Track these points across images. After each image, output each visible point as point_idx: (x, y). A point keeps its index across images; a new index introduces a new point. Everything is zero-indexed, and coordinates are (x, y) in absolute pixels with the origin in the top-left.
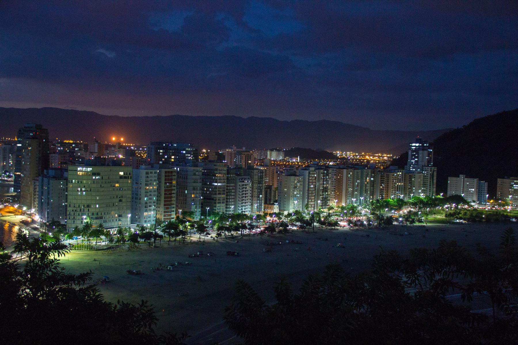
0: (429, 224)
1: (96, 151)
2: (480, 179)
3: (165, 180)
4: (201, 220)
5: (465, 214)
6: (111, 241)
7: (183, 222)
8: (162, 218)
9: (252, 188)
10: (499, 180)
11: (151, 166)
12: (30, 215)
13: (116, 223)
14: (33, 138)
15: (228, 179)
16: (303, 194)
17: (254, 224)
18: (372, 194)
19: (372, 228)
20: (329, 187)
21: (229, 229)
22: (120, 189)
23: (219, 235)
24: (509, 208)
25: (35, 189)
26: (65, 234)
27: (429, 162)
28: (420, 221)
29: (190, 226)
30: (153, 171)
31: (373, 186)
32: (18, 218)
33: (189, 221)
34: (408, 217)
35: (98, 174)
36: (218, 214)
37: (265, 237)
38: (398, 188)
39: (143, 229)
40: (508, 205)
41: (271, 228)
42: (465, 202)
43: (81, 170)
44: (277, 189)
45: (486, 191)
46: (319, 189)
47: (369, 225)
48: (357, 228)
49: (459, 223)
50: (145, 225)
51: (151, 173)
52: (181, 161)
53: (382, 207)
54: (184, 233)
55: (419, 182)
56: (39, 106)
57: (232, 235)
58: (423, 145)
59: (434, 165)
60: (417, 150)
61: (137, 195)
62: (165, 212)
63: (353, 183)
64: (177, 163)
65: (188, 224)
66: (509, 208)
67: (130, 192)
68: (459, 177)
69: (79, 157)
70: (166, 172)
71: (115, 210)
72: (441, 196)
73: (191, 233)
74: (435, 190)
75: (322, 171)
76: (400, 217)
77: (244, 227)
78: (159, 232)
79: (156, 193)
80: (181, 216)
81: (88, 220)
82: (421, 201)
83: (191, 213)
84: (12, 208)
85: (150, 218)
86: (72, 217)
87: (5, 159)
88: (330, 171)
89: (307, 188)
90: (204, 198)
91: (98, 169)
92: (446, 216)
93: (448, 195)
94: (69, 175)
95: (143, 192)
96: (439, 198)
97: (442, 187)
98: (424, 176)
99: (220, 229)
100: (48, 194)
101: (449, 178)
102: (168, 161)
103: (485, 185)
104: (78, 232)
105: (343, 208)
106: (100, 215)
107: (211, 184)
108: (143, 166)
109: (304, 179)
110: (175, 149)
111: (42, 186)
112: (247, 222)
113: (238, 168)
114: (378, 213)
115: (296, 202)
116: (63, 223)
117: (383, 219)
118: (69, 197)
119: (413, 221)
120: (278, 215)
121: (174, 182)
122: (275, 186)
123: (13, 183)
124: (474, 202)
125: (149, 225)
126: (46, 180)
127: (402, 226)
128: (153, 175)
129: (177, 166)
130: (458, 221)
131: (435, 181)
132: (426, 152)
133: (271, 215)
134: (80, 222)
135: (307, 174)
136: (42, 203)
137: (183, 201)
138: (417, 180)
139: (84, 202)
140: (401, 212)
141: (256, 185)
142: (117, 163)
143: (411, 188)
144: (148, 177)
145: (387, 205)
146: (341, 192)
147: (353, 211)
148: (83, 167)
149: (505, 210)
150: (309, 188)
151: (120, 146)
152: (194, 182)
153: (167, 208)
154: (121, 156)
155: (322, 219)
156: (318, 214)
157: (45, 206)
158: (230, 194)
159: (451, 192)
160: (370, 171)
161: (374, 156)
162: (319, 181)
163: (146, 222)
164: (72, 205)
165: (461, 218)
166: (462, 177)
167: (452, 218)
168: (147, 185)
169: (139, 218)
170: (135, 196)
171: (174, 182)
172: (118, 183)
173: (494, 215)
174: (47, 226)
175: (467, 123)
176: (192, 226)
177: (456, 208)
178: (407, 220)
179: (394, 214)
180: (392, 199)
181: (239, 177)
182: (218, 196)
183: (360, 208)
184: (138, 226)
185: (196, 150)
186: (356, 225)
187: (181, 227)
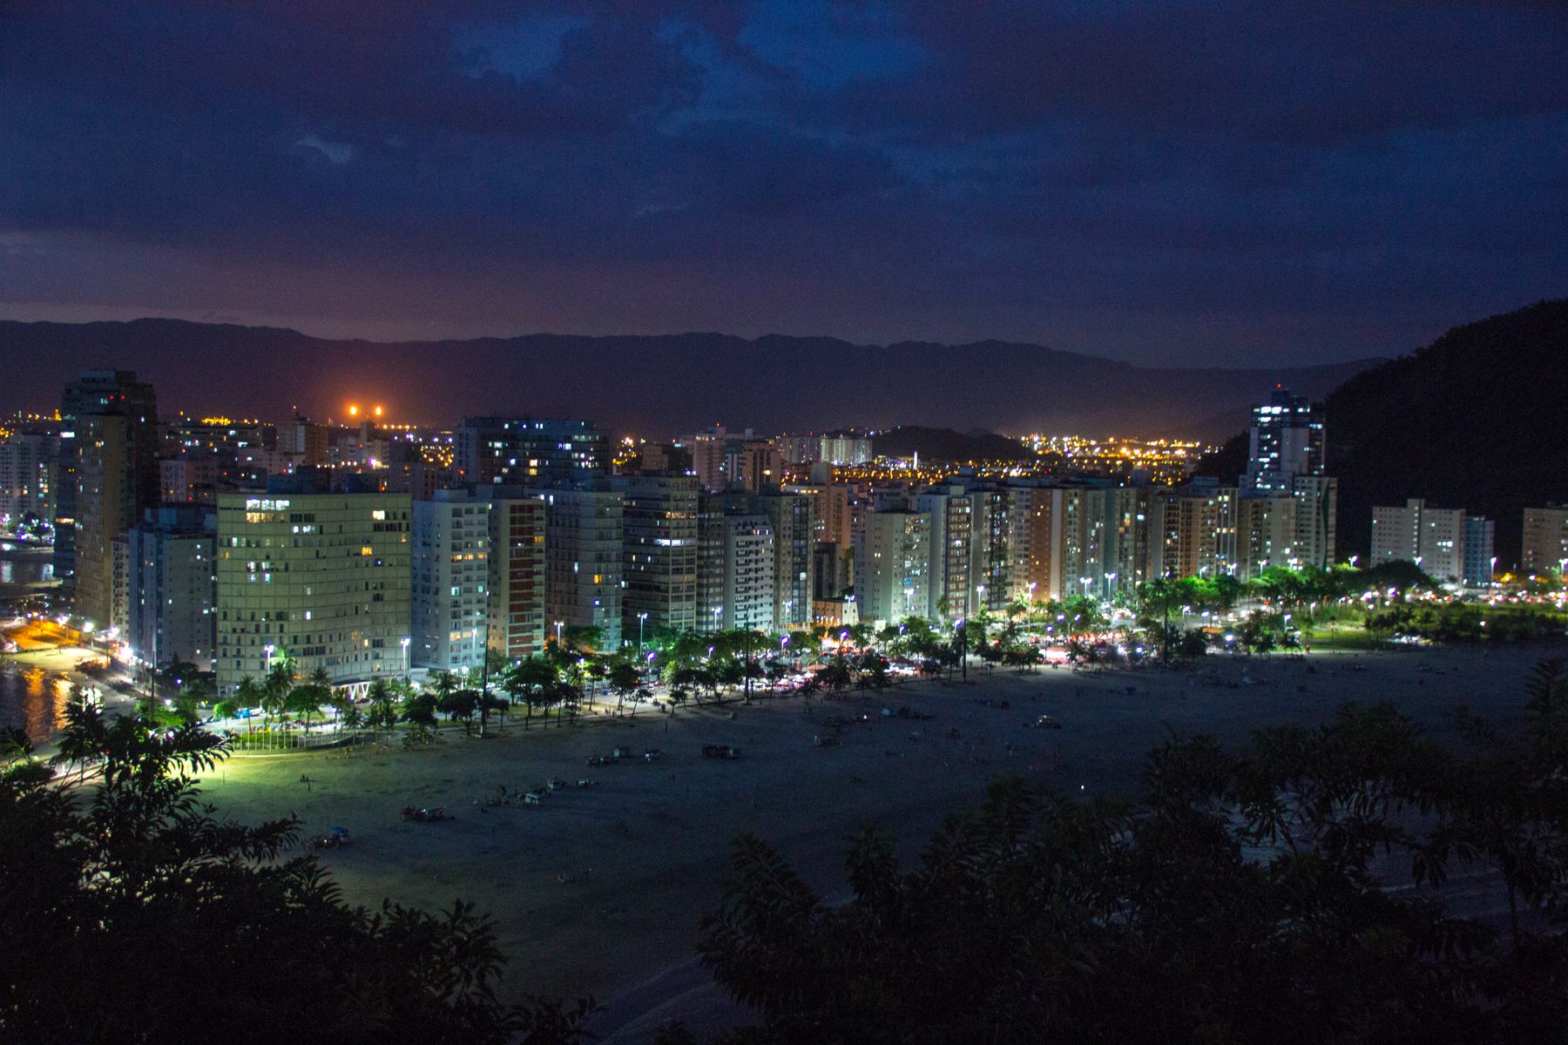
0: (1314, 652)
1: (302, 449)
2: (1471, 513)
3: (513, 532)
4: (622, 651)
5: (1427, 618)
6: (352, 719)
7: (568, 659)
8: (506, 648)
9: (777, 550)
10: (1529, 515)
11: (469, 489)
12: (106, 647)
13: (366, 667)
14: (110, 411)
15: (701, 526)
16: (932, 568)
17: (785, 660)
18: (1142, 562)
19: (1142, 667)
21: (707, 679)
22: (374, 561)
23: (678, 696)
25: (118, 566)
26: (213, 702)
27: (1313, 461)
28: (1289, 643)
29: (590, 669)
30: (475, 506)
31: (1144, 539)
32: (68, 658)
33: (588, 657)
34: (1249, 632)
35: (309, 519)
36: (674, 631)
37: (819, 696)
38: (1221, 545)
39: (447, 681)
40: (1557, 588)
41: (836, 672)
43: (257, 507)
44: (851, 552)
45: (1489, 548)
46: (978, 553)
47: (1134, 657)
48: (1096, 666)
49: (1409, 645)
50: (454, 671)
51: (469, 511)
52: (560, 473)
53: (1172, 602)
54: (572, 692)
56: (126, 315)
57: (718, 695)
58: (1294, 413)
59: (1328, 472)
60: (1276, 427)
61: (426, 578)
62: (512, 630)
63: (1084, 533)
64: (546, 481)
65: (582, 664)
67: (406, 572)
68: (1404, 505)
69: (249, 469)
70: (513, 509)
71: (361, 628)
72: (1350, 565)
73: (593, 692)
74: (1332, 546)
75: (987, 496)
76: (1228, 630)
77: (754, 670)
78: (496, 690)
79: (485, 573)
80: (561, 642)
81: (281, 658)
82: (1291, 583)
83: (593, 633)
84: (50, 626)
85: (468, 647)
86: (232, 651)
87: (25, 477)
88: (1012, 496)
89: (942, 550)
90: (631, 587)
91: (308, 503)
92: (1367, 625)
93: (1373, 563)
94: (222, 522)
95: (444, 570)
96: (1347, 573)
97: (1353, 536)
98: (1299, 506)
99: (681, 677)
100: (160, 582)
101: (1376, 510)
102: (518, 474)
103: (1485, 528)
104: (249, 695)
105: (1053, 608)
106: (315, 643)
107: (650, 543)
108: (445, 493)
109: (933, 522)
110: (539, 437)
111: (140, 557)
112: (763, 655)
113: (732, 491)
114: (1160, 620)
115: (910, 592)
116: (205, 668)
117: (1177, 640)
118: (222, 590)
119: (1267, 644)
120: (856, 632)
121: (539, 539)
122: (847, 543)
123: (51, 550)
124: (1453, 580)
125: (465, 670)
126: (149, 539)
127: (1234, 659)
128: (475, 518)
129: (548, 488)
130: (1404, 640)
131: (1332, 521)
132: (1303, 433)
133: (835, 633)
134: (255, 664)
135: (943, 507)
136: (140, 608)
137: (568, 598)
138: (1278, 516)
139: (268, 604)
140: (1231, 617)
141: (786, 544)
142: (364, 484)
143: (1259, 544)
144: (458, 525)
145: (1188, 595)
146: (1045, 557)
147: (1085, 615)
148: (261, 497)
149: (1549, 605)
150: (948, 548)
151: (372, 432)
152: (601, 538)
153: (520, 619)
154: (376, 463)
155: (992, 643)
156: (978, 627)
157: (150, 619)
158: (708, 573)
159: (1383, 552)
160: (1133, 492)
162: (978, 527)
163: (455, 660)
164: (232, 615)
165: (1413, 632)
166: (1414, 505)
167: (1386, 631)
168: (456, 549)
169: (436, 649)
170: (420, 583)
171: (539, 539)
172: (368, 543)
173: (1514, 620)
174: (156, 678)
176: (597, 671)
177: (1399, 599)
178: (1248, 640)
179: (1212, 622)
180: (1201, 577)
181: (733, 521)
182: (674, 578)
183: (1104, 606)
184: (432, 673)
185: (604, 440)
186: (1093, 658)
187: (563, 676)
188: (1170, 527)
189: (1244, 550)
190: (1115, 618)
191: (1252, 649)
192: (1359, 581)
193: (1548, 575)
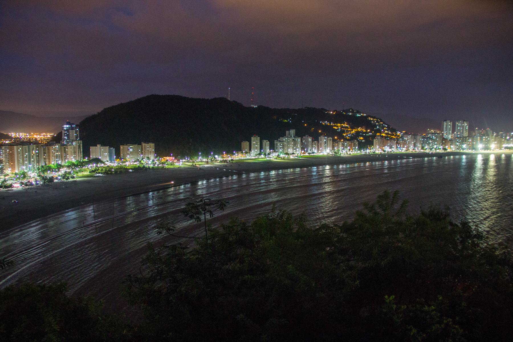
5: (102, 170)
18: (38, 162)
20: (4, 160)
27: (77, 137)
28: (73, 177)
34: (64, 176)
38: (57, 157)
40: (127, 161)
42: (102, 162)
47: (37, 184)
48: (28, 187)
55: (71, 151)
60: (67, 130)
63: (23, 156)
68: (96, 146)
72: (86, 160)
76: (59, 176)
82: (73, 164)
88: (3, 148)
92: (90, 172)
93: (91, 159)
97: (86, 153)
101: (91, 147)
103: (113, 150)
105: (16, 174)
117: (47, 179)
119: (68, 178)
124: (107, 161)
130: (98, 175)
131: (82, 150)
132: (74, 131)
138: (69, 150)
145: (50, 169)
160: (35, 146)
161: (40, 135)
165: (99, 173)
166: (99, 146)
173: (119, 169)
175: (100, 110)
177: (97, 166)
178: (64, 178)
179: (55, 175)
183: (30, 173)
186: (26, 185)
188: (45, 153)
190: (32, 175)
193: (125, 159)
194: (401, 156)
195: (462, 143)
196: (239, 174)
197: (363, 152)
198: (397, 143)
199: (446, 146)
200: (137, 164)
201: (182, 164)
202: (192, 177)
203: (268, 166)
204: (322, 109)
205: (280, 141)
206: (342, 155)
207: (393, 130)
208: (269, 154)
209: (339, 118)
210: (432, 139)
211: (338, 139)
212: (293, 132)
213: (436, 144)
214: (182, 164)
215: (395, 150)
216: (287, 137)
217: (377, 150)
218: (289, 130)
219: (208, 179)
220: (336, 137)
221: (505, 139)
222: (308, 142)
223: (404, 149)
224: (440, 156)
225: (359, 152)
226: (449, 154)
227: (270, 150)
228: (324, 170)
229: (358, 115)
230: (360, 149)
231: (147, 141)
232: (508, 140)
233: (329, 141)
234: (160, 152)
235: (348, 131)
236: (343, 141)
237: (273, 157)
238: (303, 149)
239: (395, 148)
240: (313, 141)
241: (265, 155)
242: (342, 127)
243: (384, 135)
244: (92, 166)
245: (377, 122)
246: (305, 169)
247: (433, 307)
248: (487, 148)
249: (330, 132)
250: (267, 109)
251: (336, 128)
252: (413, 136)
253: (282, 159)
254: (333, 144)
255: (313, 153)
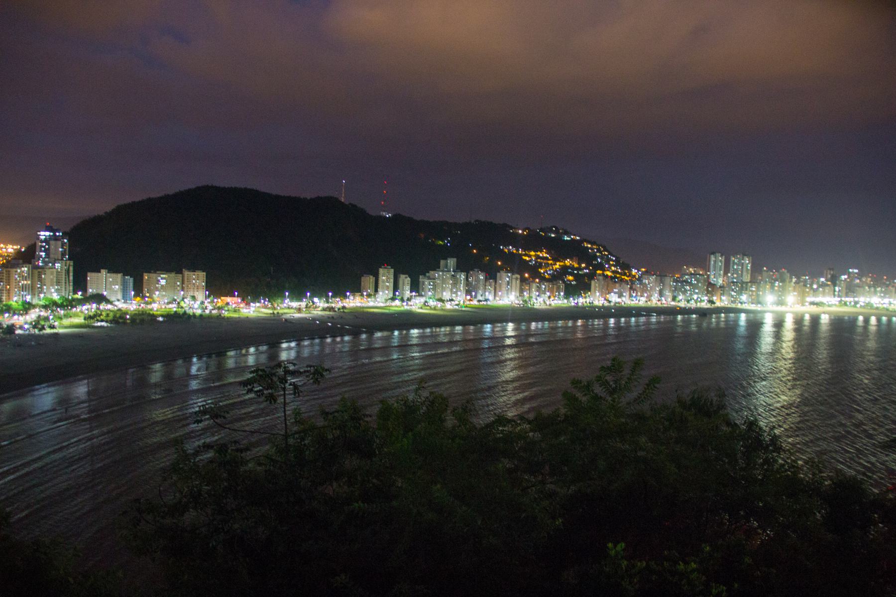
0: (61, 331)
2: (124, 275)
5: (108, 315)
24: (155, 306)
27: (63, 254)
28: (52, 327)
34: (36, 324)
38: (24, 288)
55: (52, 280)
58: (55, 235)
59: (70, 259)
60: (46, 241)
66: (155, 306)
72: (79, 295)
74: (71, 288)
76: (26, 323)
82: (55, 304)
92: (85, 319)
93: (88, 294)
96: (78, 299)
97: (80, 283)
98: (57, 272)
101: (89, 274)
103: (130, 280)
119: (43, 328)
124: (118, 300)
130: (99, 324)
131: (71, 278)
132: (59, 243)
165: (102, 321)
166: (104, 272)
173: (139, 315)
177: (98, 309)
179: (18, 320)
189: (32, 290)
191: (37, 331)
192: (82, 302)
194: (638, 312)
195: (740, 293)
196: (355, 333)
197: (572, 302)
198: (631, 288)
199: (713, 295)
200: (173, 308)
201: (254, 310)
202: (273, 332)
203: (407, 321)
204: (506, 226)
205: (429, 278)
206: (537, 306)
207: (626, 267)
208: (409, 299)
209: (533, 241)
210: (690, 284)
211: (530, 276)
212: (452, 262)
213: (697, 293)
214: (254, 310)
215: (628, 300)
216: (443, 271)
217: (595, 299)
218: (446, 259)
219: (299, 340)
220: (529, 274)
221: (811, 288)
222: (478, 280)
223: (643, 299)
224: (703, 313)
225: (566, 301)
226: (718, 310)
227: (411, 292)
228: (504, 330)
229: (566, 238)
230: (567, 296)
231: (193, 268)
232: (815, 291)
233: (514, 281)
234: (215, 288)
235: (547, 265)
236: (539, 283)
237: (417, 305)
238: (468, 292)
239: (628, 297)
240: (486, 279)
241: (402, 300)
242: (538, 257)
243: (609, 274)
244: (90, 308)
245: (599, 250)
246: (472, 327)
247: (694, 565)
248: (781, 303)
249: (517, 266)
250: (410, 220)
251: (527, 258)
252: (659, 278)
253: (431, 309)
254: (521, 285)
255: (486, 300)
